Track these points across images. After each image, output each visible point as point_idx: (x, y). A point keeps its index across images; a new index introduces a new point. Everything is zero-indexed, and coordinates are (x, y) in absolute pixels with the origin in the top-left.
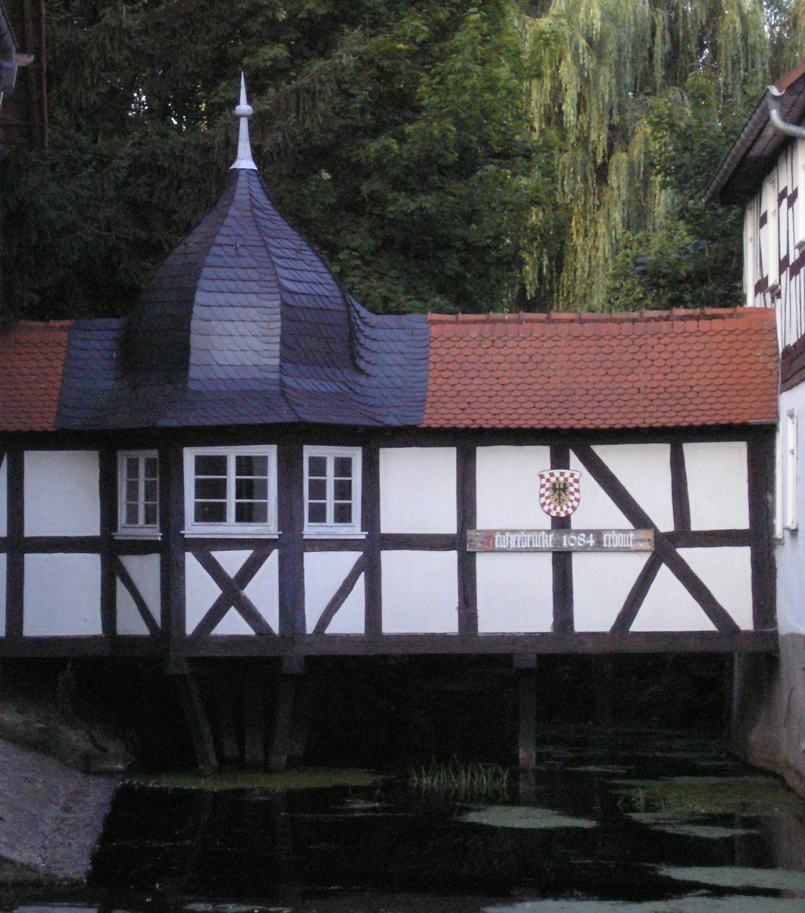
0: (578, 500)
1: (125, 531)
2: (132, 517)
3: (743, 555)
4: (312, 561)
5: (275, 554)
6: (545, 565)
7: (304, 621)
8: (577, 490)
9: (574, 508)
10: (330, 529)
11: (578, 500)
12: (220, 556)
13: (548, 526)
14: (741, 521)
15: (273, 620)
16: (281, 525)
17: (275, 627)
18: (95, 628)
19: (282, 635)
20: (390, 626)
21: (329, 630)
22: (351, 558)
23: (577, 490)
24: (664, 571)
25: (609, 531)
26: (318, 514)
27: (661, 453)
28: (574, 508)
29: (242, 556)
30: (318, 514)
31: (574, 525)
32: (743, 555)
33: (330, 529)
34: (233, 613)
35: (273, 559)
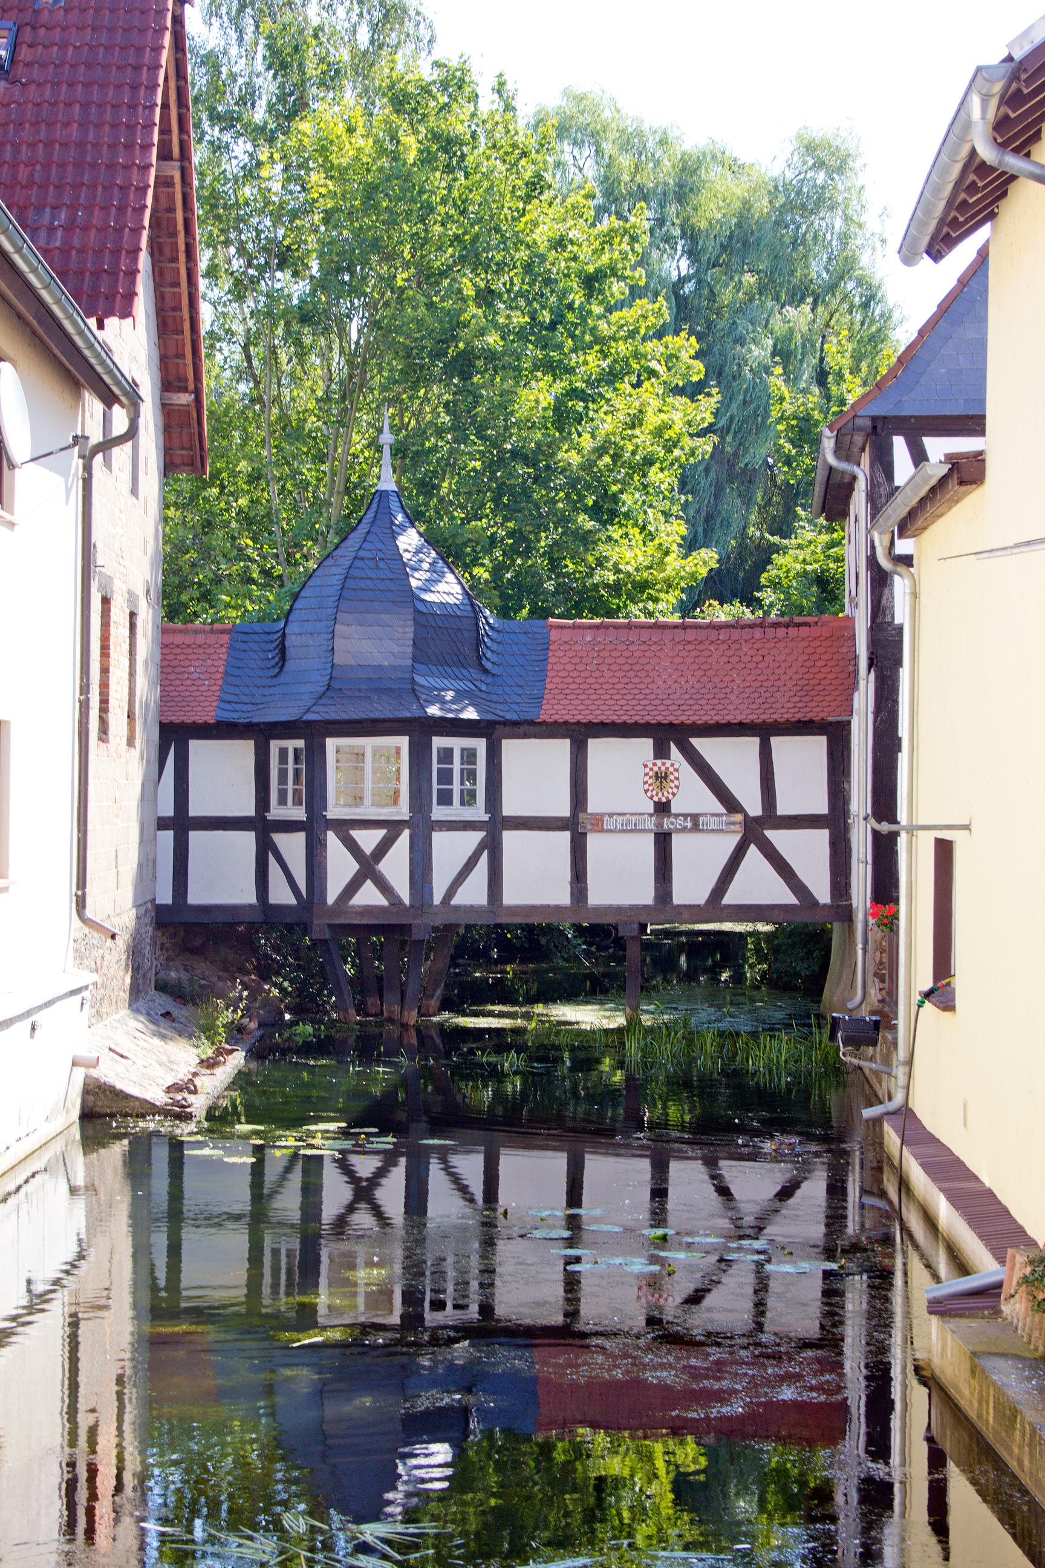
0: (677, 787)
1: (276, 812)
2: (283, 801)
3: (822, 836)
4: (439, 838)
5: (406, 834)
6: (648, 843)
7: (431, 894)
8: (677, 779)
9: (674, 794)
10: (455, 812)
11: (677, 787)
12: (357, 834)
13: (652, 811)
14: (820, 806)
15: (404, 893)
16: (412, 808)
17: (406, 900)
18: (249, 897)
19: (412, 906)
20: (511, 897)
21: (454, 902)
22: (475, 838)
23: (677, 779)
24: (753, 850)
25: (706, 815)
26: (445, 799)
27: (752, 744)
28: (674, 794)
29: (377, 835)
30: (445, 799)
31: (674, 809)
32: (822, 836)
33: (455, 812)
34: (369, 885)
35: (404, 839)
